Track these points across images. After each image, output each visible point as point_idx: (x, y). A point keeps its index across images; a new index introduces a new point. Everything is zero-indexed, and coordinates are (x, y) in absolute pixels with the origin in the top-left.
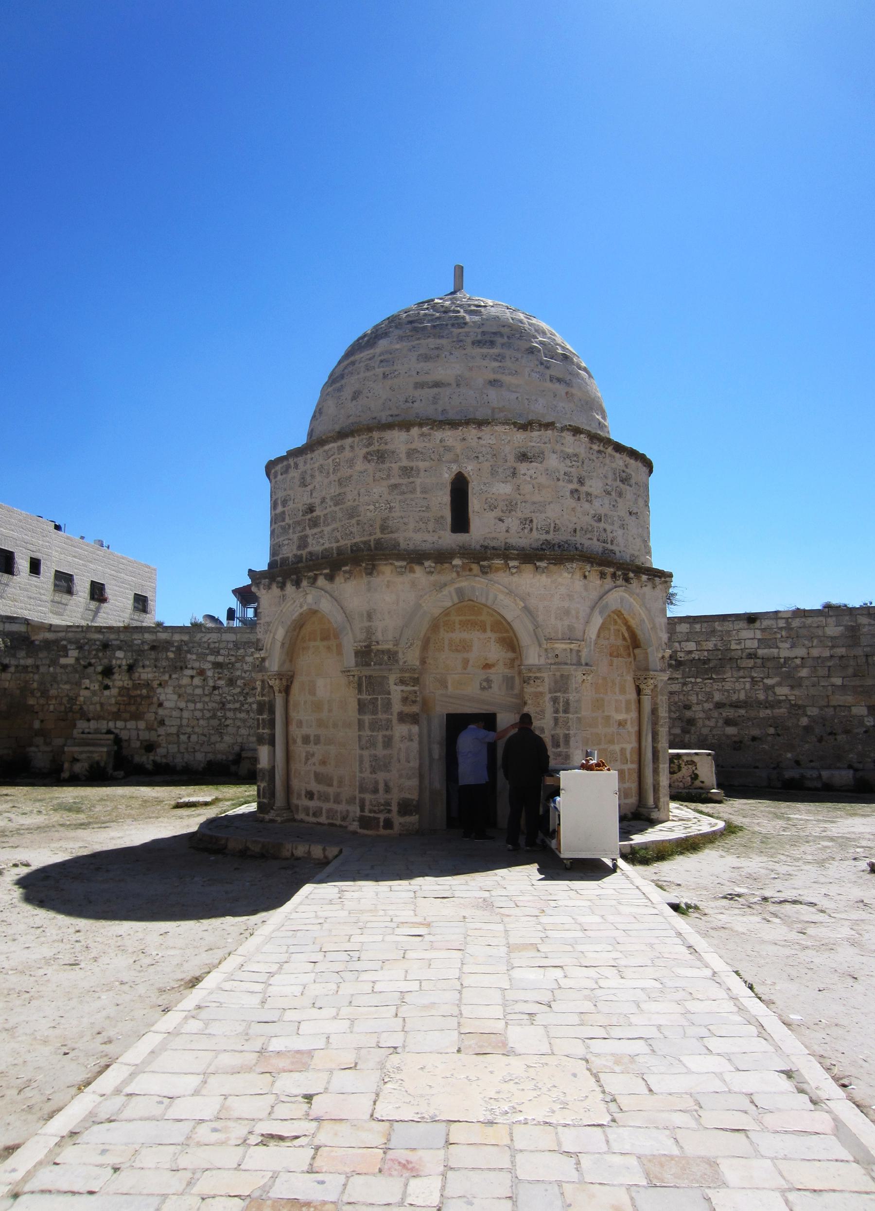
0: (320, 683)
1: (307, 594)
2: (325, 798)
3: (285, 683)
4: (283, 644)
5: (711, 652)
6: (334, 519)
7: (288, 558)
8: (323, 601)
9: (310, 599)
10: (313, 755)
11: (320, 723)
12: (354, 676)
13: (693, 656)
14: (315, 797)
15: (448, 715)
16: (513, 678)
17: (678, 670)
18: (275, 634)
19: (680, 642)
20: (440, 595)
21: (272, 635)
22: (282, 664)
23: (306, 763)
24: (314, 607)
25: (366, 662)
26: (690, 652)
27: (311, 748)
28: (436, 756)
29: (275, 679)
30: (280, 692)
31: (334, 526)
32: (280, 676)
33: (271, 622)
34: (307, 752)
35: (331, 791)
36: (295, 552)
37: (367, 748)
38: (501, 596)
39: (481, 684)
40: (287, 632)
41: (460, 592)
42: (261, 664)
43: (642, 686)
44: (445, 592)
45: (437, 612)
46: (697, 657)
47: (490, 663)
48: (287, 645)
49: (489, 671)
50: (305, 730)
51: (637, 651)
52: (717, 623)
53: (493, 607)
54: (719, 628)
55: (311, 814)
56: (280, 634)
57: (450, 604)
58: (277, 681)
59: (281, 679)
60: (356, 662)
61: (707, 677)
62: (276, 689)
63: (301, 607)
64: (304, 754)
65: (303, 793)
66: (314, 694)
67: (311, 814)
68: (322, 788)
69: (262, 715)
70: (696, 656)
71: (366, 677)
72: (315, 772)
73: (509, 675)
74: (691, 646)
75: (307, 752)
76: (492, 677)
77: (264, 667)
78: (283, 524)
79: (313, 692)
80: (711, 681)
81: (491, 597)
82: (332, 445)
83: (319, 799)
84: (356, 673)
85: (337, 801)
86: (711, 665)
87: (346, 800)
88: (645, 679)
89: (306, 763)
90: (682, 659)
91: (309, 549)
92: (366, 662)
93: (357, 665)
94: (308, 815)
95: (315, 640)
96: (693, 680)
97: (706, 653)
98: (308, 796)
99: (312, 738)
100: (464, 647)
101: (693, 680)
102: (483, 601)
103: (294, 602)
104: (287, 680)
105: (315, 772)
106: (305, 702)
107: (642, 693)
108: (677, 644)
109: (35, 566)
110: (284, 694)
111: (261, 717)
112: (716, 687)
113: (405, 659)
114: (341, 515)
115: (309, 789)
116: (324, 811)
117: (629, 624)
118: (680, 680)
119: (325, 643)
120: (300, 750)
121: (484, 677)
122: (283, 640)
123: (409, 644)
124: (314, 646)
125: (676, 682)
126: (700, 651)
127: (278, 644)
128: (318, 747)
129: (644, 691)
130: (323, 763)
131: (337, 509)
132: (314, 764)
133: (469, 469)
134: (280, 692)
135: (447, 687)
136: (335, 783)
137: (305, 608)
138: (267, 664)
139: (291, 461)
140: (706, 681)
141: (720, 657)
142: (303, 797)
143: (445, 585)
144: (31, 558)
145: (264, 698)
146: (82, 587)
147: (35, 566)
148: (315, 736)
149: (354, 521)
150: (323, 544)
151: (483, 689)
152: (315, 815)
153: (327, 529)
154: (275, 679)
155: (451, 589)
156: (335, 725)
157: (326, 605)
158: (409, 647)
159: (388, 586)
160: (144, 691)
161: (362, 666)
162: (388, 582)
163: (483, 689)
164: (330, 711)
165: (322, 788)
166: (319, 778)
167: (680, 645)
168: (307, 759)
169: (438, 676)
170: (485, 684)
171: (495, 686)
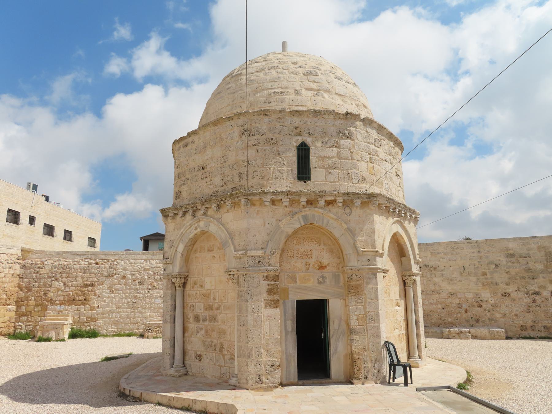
0: (207, 280)
1: (200, 221)
3: (183, 281)
4: (182, 254)
8: (212, 225)
9: (202, 224)
12: (234, 274)
15: (298, 302)
16: (339, 275)
18: (177, 248)
20: (292, 220)
21: (175, 248)
22: (181, 268)
24: (205, 229)
27: (201, 324)
28: (290, 329)
29: (177, 278)
30: (180, 287)
32: (179, 275)
33: (175, 240)
38: (331, 221)
39: (318, 280)
40: (185, 247)
41: (305, 217)
43: (406, 281)
44: (296, 217)
45: (290, 231)
47: (323, 265)
48: (185, 255)
49: (324, 271)
51: (403, 259)
53: (327, 228)
56: (181, 248)
57: (299, 226)
58: (178, 279)
59: (180, 278)
62: (177, 285)
63: (196, 229)
73: (336, 273)
76: (326, 275)
81: (325, 221)
84: (235, 273)
88: (409, 276)
100: (307, 255)
102: (320, 224)
103: (191, 226)
104: (185, 278)
107: (407, 285)
109: (32, 220)
110: (182, 288)
113: (270, 263)
117: (400, 242)
120: (192, 326)
121: (320, 275)
122: (183, 252)
123: (272, 252)
127: (179, 255)
129: (408, 284)
133: (309, 141)
134: (180, 287)
135: (296, 282)
137: (198, 230)
139: (190, 139)
143: (296, 213)
144: (30, 216)
146: (59, 233)
147: (32, 220)
151: (320, 283)
154: (177, 278)
155: (299, 216)
157: (213, 228)
158: (272, 255)
159: (257, 213)
160: (90, 288)
162: (258, 211)
163: (320, 283)
169: (290, 274)
170: (321, 279)
171: (327, 281)
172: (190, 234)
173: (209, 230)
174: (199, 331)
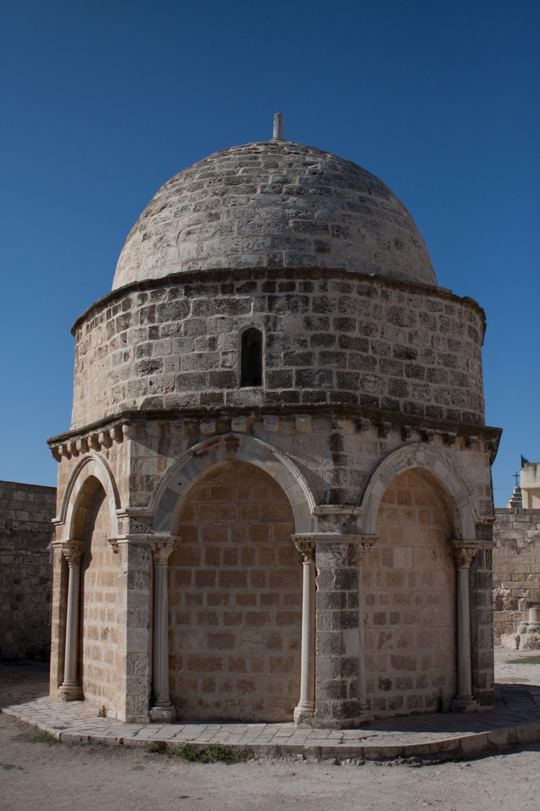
2: (408, 685)
5: (41, 525)
6: (444, 379)
7: (376, 399)
10: (390, 636)
11: (399, 599)
13: (26, 527)
14: (393, 685)
17: (11, 541)
19: (16, 510)
23: (380, 647)
25: (487, 536)
26: (23, 522)
27: (387, 628)
31: (443, 385)
34: (382, 634)
35: (413, 675)
36: (386, 394)
37: (488, 623)
42: (350, 523)
46: (29, 529)
50: (378, 608)
52: (47, 496)
54: (49, 501)
55: (387, 707)
60: (477, 534)
61: (35, 550)
64: (378, 636)
65: (377, 683)
66: (391, 565)
67: (387, 707)
68: (402, 674)
69: (349, 588)
70: (28, 527)
71: (487, 551)
72: (392, 657)
74: (25, 516)
75: (382, 634)
77: (355, 527)
78: (365, 354)
79: (389, 562)
80: (39, 555)
82: (438, 300)
83: (398, 687)
85: (421, 684)
86: (40, 538)
87: (433, 682)
89: (380, 647)
90: (17, 529)
91: (409, 399)
92: (487, 536)
93: (478, 538)
94: (384, 709)
95: (392, 502)
96: (23, 552)
97: (36, 525)
98: (383, 687)
99: (388, 616)
101: (23, 552)
105: (392, 657)
106: (379, 574)
108: (13, 513)
111: (347, 592)
112: (42, 561)
114: (452, 378)
115: (384, 678)
116: (405, 700)
118: (13, 552)
119: (404, 507)
124: (389, 509)
125: (9, 553)
126: (32, 522)
128: (396, 626)
130: (403, 644)
131: (447, 369)
132: (391, 647)
136: (419, 666)
138: (359, 523)
140: (35, 555)
141: (48, 530)
142: (376, 688)
145: (353, 567)
148: (391, 614)
149: (464, 389)
150: (429, 400)
152: (392, 707)
153: (433, 386)
156: (418, 601)
161: (483, 539)
164: (412, 585)
165: (402, 674)
166: (397, 662)
167: (16, 514)
168: (381, 642)
172: (398, 470)
173: (433, 470)
174: (385, 639)
